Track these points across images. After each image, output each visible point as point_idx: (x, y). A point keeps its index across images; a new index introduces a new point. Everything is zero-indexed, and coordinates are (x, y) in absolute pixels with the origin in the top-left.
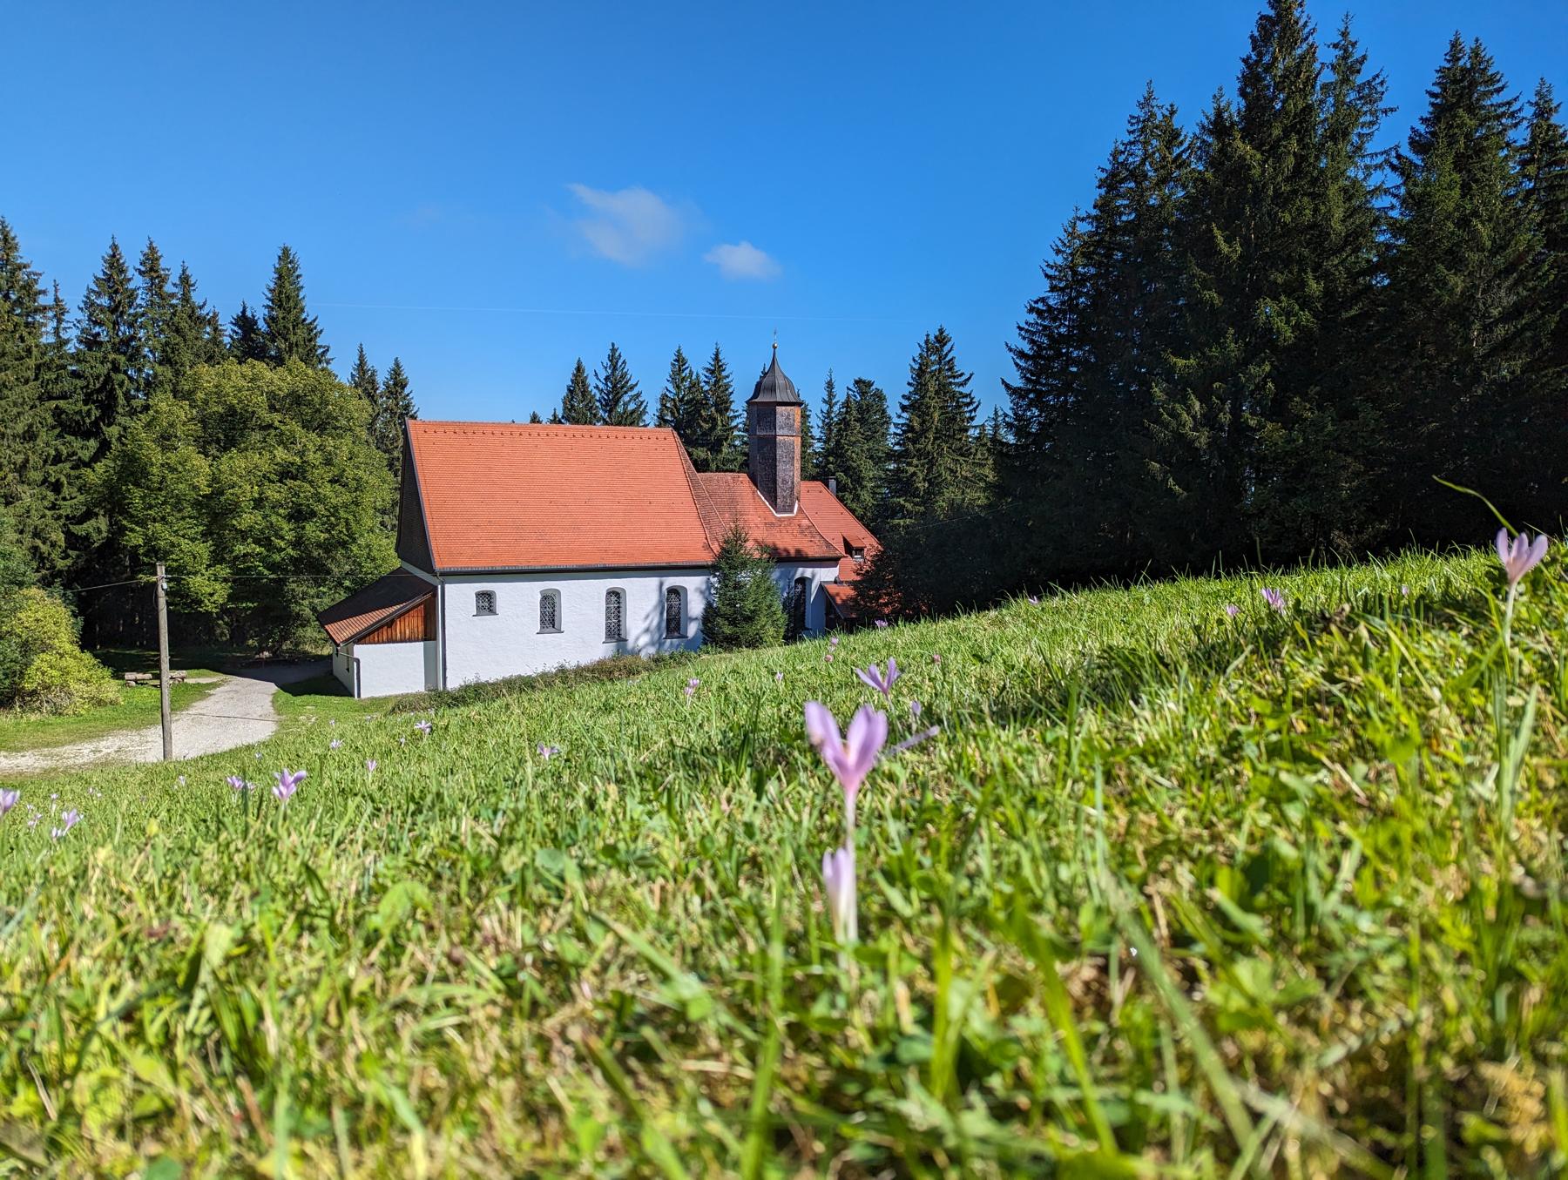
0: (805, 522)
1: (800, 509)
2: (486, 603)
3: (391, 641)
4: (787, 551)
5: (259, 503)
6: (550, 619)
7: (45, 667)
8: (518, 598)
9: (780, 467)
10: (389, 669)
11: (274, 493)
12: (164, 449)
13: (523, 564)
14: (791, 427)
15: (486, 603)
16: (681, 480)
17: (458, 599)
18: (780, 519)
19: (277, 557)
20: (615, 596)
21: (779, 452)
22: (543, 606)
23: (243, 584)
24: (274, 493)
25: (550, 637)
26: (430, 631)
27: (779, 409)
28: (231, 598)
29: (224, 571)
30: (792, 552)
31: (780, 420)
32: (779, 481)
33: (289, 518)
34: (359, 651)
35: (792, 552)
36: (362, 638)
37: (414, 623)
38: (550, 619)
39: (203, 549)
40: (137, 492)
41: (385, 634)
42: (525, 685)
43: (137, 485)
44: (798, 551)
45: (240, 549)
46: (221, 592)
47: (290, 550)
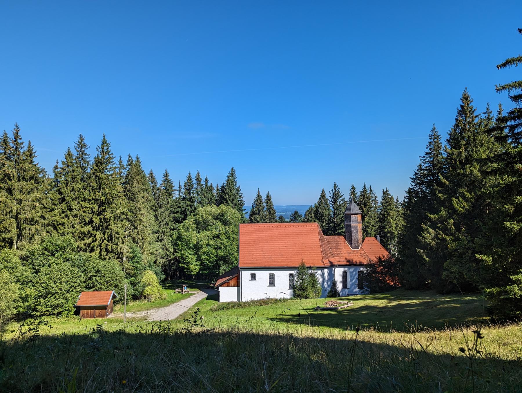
0: (363, 252)
1: (361, 248)
2: (253, 277)
3: (228, 286)
4: (356, 262)
5: (208, 245)
6: (272, 282)
7: (149, 290)
8: (263, 276)
9: (353, 234)
10: (227, 294)
11: (211, 242)
12: (186, 231)
13: (263, 266)
14: (357, 221)
15: (253, 277)
16: (317, 239)
17: (245, 275)
18: (353, 251)
19: (211, 260)
20: (272, 277)
21: (352, 229)
22: (270, 278)
23: (204, 266)
24: (211, 242)
25: (272, 288)
26: (238, 285)
27: (352, 216)
28: (200, 269)
29: (199, 263)
30: (358, 263)
31: (352, 219)
32: (353, 239)
33: (215, 249)
34: (220, 289)
35: (358, 263)
36: (221, 285)
37: (234, 282)
38: (272, 282)
39: (194, 257)
40: (180, 243)
41: (227, 284)
42: (276, 301)
43: (180, 241)
44: (360, 262)
45: (203, 257)
46: (198, 268)
47: (215, 258)
